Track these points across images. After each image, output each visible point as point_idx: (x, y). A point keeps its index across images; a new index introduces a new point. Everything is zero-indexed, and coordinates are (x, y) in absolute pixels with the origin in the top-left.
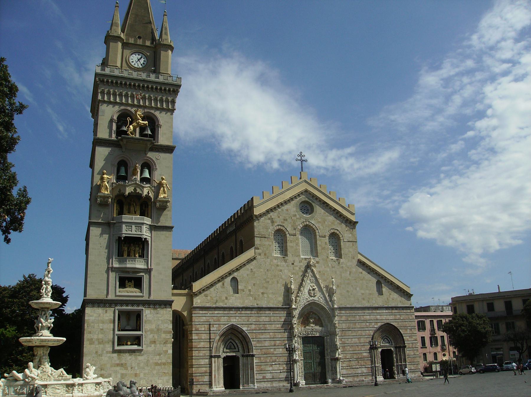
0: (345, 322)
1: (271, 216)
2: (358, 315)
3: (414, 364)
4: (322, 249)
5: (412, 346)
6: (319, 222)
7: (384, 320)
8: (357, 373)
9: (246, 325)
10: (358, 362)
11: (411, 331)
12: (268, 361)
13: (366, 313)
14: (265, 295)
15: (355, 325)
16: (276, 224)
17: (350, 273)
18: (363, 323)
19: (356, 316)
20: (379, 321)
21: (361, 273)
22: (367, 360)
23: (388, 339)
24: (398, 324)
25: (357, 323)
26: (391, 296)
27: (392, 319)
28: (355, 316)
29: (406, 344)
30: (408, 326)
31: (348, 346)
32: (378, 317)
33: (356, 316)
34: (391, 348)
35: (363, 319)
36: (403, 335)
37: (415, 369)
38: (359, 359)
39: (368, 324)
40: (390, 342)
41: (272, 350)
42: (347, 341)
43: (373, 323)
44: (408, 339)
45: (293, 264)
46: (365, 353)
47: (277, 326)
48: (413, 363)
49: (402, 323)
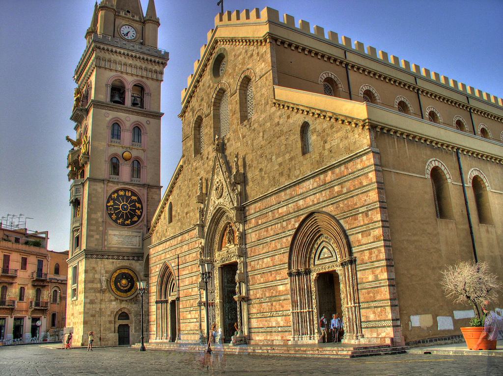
0: (255, 229)
1: (192, 105)
2: (271, 211)
3: (375, 307)
4: (233, 115)
5: (370, 258)
6: (230, 75)
7: (311, 206)
8: (270, 326)
9: (173, 261)
10: (272, 305)
11: (367, 215)
12: (188, 306)
13: (282, 203)
14: (188, 215)
15: (267, 231)
16: (195, 112)
17: (263, 134)
18: (278, 223)
19: (267, 214)
20: (301, 212)
21: (278, 124)
22: (284, 300)
23: (330, 248)
24: (337, 207)
25: (270, 226)
26: (327, 146)
27: (325, 199)
28: (267, 213)
29: (355, 255)
30: (358, 205)
31: (259, 274)
32: (301, 203)
33: (269, 212)
34: (335, 269)
35: (277, 216)
36: (349, 233)
37: (379, 321)
38: (273, 299)
39: (284, 223)
40: (334, 254)
41: (190, 290)
42: (257, 264)
43: (293, 220)
44: (359, 241)
45: (207, 158)
46: (281, 286)
47: (194, 255)
48: (373, 304)
49: (346, 202)
